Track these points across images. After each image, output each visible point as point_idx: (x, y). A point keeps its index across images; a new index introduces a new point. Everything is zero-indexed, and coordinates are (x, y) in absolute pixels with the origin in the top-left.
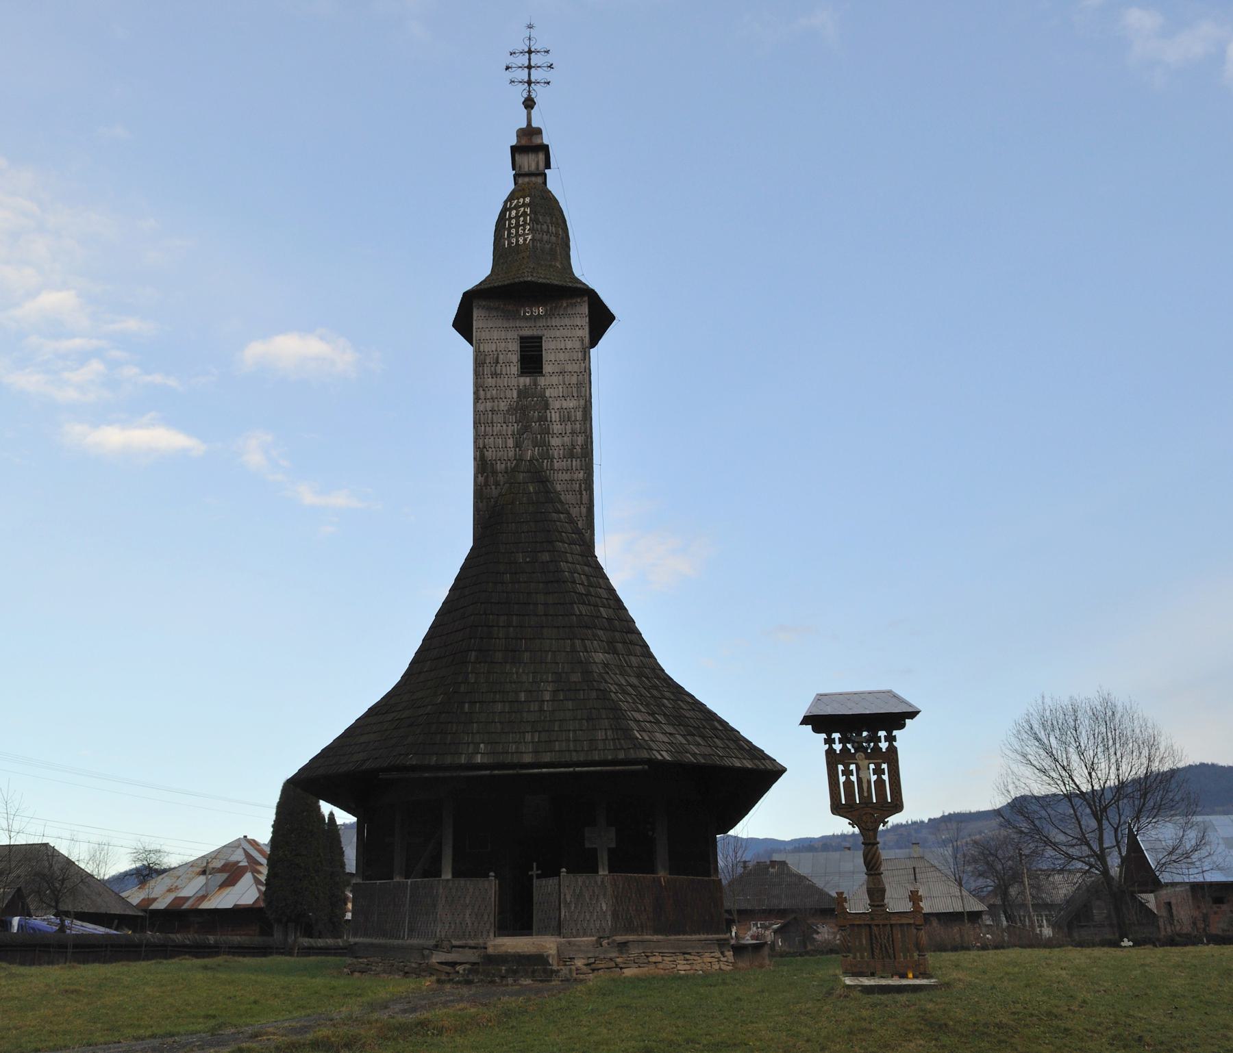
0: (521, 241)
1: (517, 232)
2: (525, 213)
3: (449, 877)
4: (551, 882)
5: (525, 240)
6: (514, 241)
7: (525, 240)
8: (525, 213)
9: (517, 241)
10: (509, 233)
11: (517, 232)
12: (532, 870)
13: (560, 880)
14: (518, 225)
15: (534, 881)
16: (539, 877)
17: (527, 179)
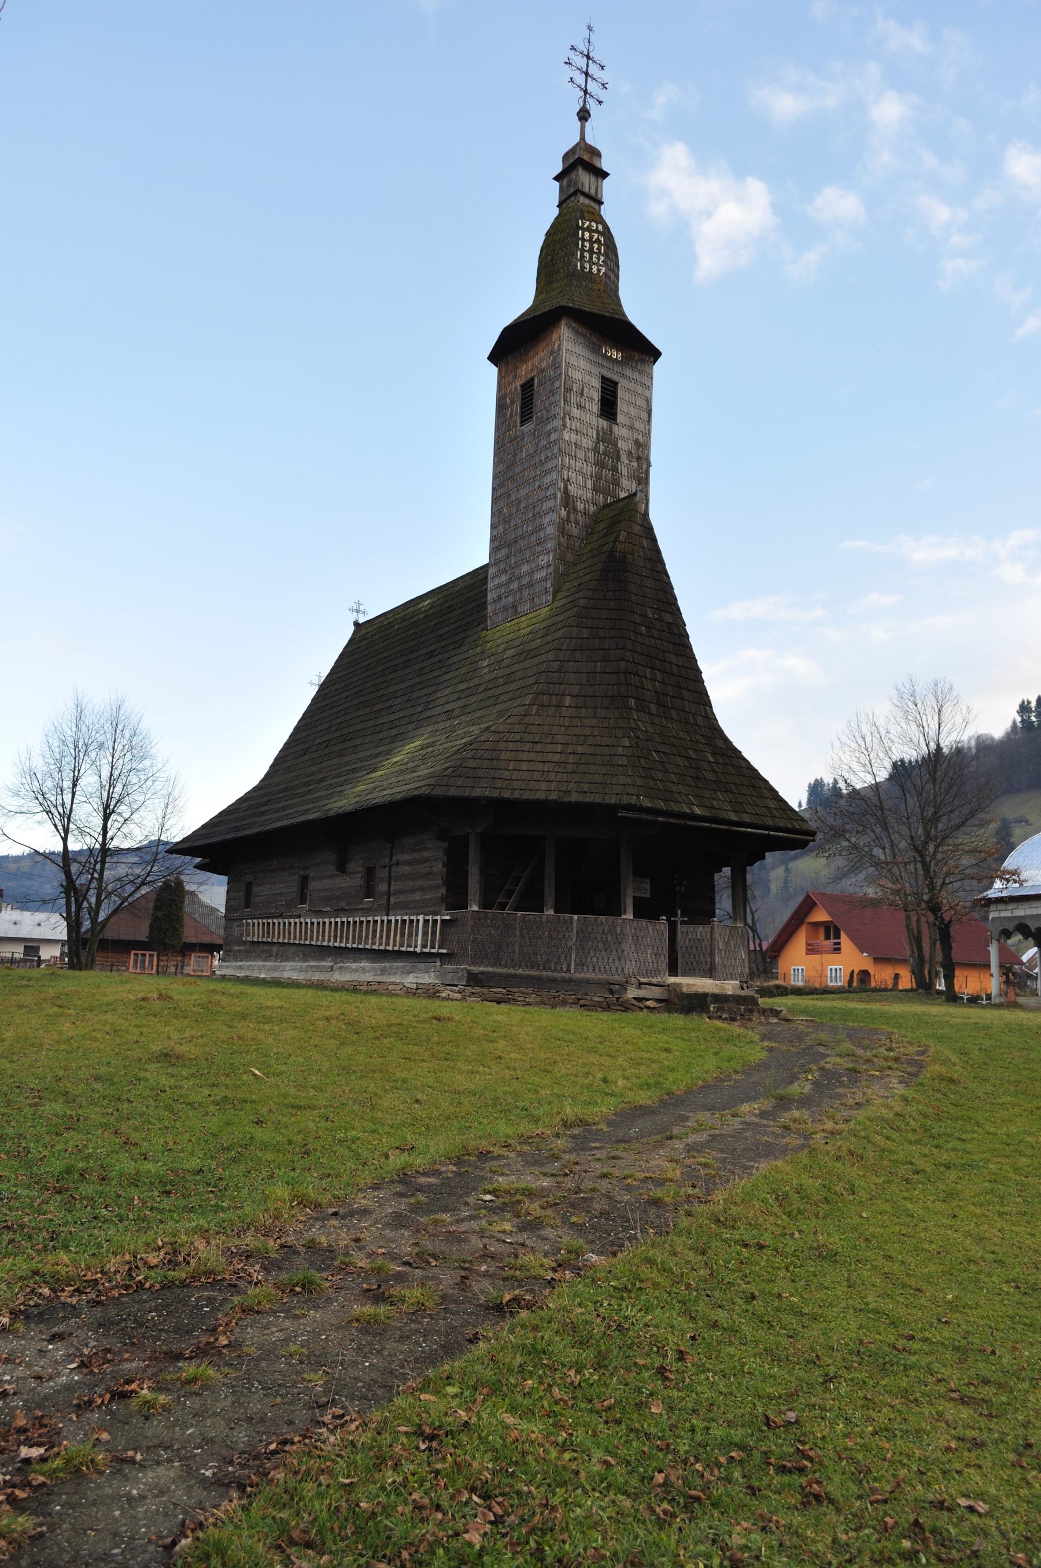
0: (595, 269)
1: (591, 258)
2: (598, 241)
3: (631, 917)
4: (700, 931)
5: (599, 271)
6: (587, 266)
7: (599, 271)
8: (598, 241)
9: (591, 269)
10: (582, 256)
11: (591, 258)
12: (676, 916)
13: (712, 928)
14: (591, 251)
15: (679, 926)
16: (683, 923)
17: (587, 201)
